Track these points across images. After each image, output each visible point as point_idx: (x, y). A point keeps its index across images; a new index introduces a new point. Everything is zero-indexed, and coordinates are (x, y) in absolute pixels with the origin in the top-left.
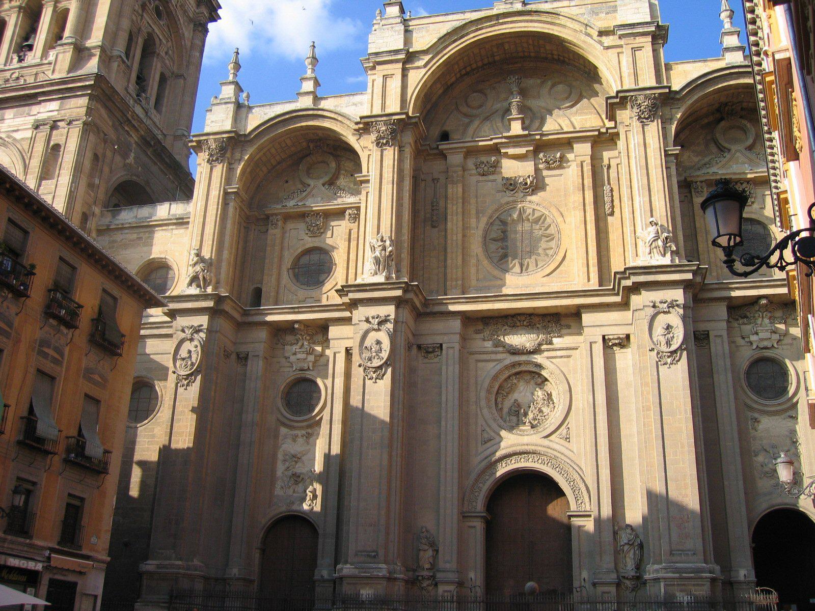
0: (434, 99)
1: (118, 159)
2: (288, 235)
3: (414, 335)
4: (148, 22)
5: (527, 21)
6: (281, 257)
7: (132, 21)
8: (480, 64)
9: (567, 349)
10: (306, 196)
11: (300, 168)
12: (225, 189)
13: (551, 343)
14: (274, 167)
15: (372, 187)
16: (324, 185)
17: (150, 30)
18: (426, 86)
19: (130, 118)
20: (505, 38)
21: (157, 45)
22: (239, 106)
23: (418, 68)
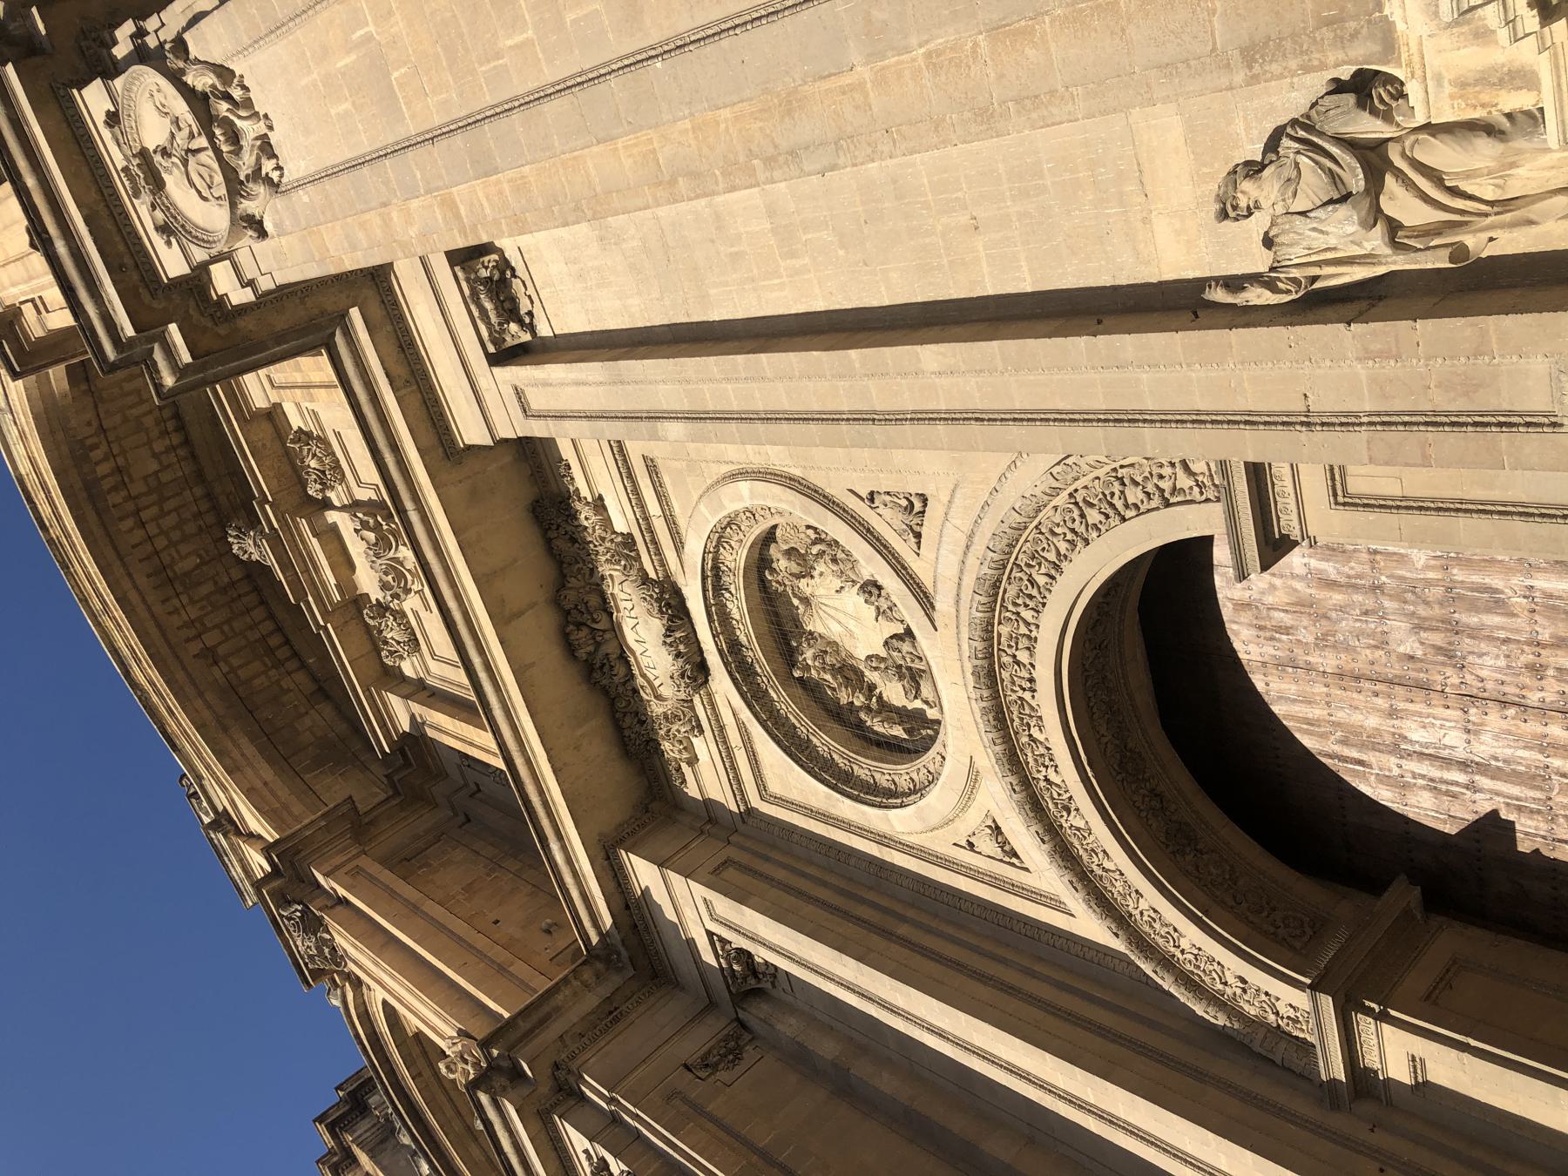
0: (342, 727)
3: (711, 1005)
5: (73, 545)
8: (259, 613)
9: (628, 474)
13: (629, 541)
18: (265, 784)
20: (136, 587)
23: (232, 803)
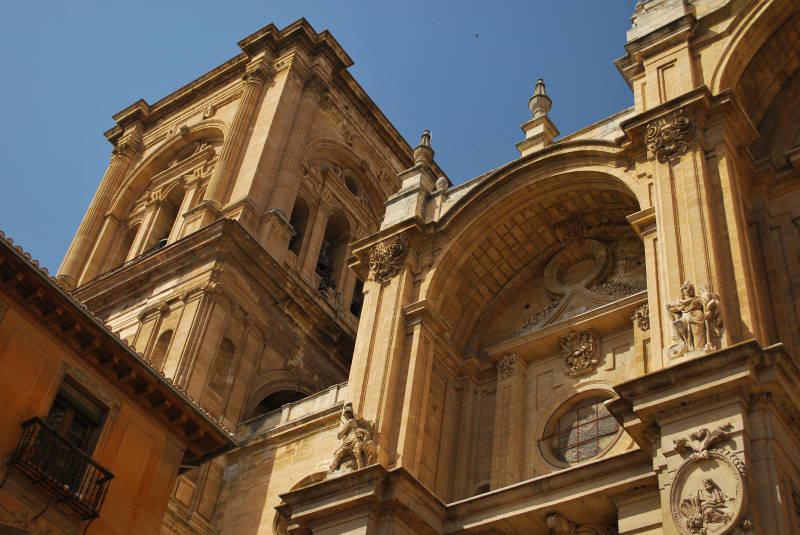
1: (271, 354)
2: (533, 385)
4: (334, 195)
6: (524, 424)
7: (303, 185)
10: (560, 313)
11: (545, 275)
12: (403, 312)
14: (502, 287)
15: (663, 231)
16: (588, 287)
17: (339, 206)
18: (740, 63)
19: (290, 293)
21: (352, 228)
22: (429, 199)
23: (719, 37)
